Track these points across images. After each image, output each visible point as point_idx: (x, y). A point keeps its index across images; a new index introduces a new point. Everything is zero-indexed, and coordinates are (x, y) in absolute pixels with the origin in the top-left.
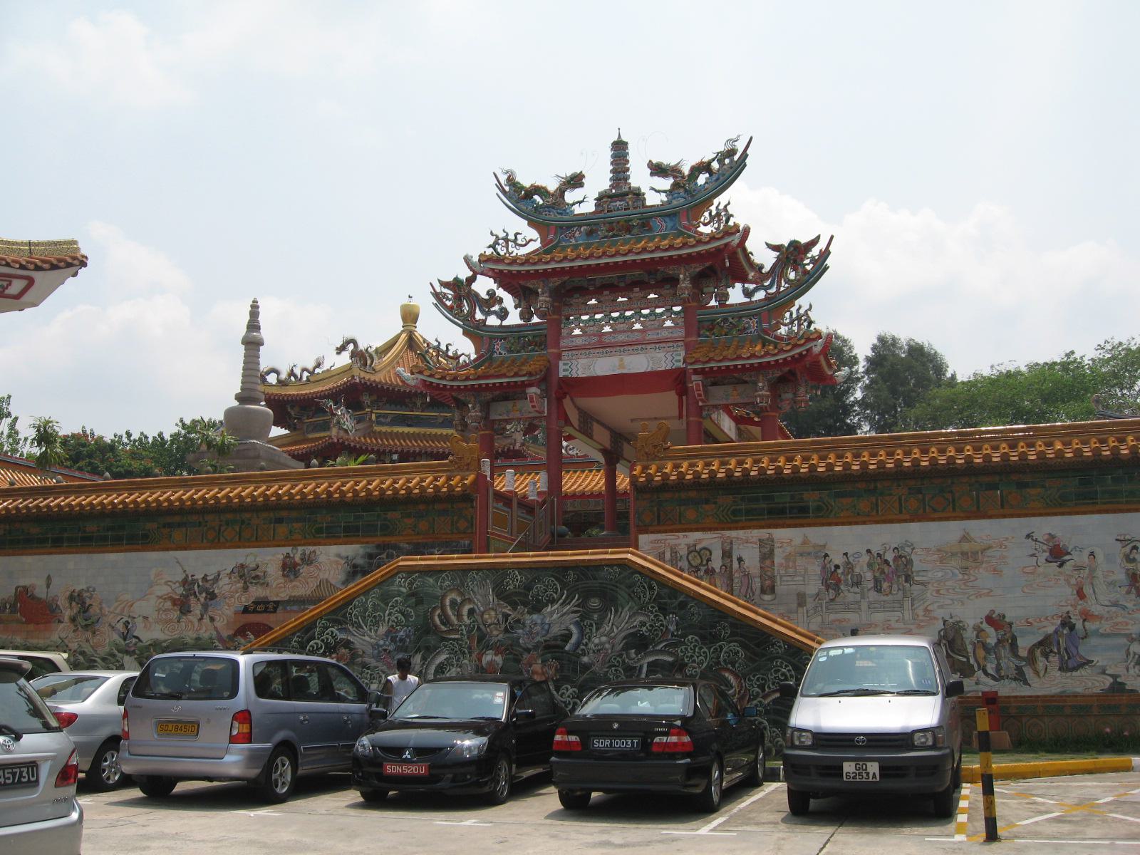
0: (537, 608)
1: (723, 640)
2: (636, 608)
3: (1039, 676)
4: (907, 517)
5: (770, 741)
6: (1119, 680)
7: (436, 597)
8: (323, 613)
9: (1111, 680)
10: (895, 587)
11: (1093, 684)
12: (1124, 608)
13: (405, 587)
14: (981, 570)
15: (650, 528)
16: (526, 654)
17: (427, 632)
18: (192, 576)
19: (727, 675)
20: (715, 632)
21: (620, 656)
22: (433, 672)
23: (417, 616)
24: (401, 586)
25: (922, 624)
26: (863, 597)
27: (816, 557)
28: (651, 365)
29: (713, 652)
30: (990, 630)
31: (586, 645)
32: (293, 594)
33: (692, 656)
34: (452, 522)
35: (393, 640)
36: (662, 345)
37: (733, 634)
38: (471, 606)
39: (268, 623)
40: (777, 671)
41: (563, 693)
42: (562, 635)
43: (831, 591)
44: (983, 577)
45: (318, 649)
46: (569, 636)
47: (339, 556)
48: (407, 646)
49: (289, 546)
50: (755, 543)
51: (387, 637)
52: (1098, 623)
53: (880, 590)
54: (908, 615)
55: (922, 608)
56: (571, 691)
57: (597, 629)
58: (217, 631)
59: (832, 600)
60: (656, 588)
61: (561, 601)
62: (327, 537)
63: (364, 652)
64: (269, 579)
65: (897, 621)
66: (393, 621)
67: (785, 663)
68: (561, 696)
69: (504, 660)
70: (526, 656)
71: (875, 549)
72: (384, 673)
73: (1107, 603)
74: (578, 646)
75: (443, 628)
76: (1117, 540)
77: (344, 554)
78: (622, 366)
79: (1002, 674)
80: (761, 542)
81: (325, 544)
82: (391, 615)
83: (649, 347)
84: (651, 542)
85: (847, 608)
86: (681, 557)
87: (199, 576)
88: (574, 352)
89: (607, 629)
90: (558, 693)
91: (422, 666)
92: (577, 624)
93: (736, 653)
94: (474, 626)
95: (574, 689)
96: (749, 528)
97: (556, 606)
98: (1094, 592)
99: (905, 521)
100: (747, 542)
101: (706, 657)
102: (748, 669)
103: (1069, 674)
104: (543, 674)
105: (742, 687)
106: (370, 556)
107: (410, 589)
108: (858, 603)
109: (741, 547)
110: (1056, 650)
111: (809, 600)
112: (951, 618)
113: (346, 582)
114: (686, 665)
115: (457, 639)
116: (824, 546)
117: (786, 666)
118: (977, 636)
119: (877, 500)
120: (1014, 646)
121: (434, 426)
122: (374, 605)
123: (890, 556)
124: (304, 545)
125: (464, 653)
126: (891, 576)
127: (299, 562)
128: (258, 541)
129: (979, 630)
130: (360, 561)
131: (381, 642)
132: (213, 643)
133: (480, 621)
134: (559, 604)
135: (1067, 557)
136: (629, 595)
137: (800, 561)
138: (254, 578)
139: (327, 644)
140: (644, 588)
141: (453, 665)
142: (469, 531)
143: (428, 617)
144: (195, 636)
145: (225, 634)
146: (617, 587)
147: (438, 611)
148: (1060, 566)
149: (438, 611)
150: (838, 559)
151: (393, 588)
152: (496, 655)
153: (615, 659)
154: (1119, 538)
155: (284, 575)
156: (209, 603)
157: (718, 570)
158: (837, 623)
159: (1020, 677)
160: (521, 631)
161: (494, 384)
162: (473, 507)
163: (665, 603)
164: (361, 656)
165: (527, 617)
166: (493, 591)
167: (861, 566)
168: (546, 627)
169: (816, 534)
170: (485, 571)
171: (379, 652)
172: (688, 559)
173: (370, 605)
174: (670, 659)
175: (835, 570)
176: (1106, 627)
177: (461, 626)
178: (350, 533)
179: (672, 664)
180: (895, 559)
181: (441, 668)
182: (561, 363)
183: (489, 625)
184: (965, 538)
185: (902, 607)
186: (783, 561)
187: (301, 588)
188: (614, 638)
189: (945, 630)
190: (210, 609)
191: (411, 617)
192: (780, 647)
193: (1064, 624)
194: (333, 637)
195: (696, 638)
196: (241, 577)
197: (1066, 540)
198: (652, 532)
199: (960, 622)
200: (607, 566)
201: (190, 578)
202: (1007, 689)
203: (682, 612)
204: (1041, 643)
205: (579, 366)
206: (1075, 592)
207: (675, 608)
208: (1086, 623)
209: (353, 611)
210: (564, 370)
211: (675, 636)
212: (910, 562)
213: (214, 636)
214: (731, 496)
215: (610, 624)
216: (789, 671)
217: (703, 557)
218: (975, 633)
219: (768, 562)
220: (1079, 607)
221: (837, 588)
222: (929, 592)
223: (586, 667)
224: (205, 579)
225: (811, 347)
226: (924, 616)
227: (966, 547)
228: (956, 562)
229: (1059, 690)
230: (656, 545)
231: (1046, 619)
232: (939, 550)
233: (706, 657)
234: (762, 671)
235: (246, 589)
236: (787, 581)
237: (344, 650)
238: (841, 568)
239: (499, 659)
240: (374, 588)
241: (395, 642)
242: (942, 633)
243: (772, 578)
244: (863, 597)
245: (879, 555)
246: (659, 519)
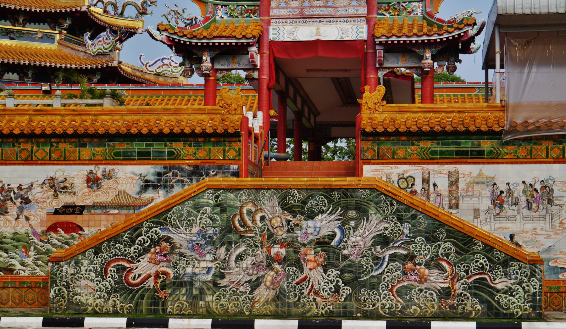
0: (311, 216)
2: (382, 218)
4: (552, 160)
5: (471, 307)
7: (237, 208)
8: (149, 217)
10: (541, 206)
13: (212, 199)
15: (372, 161)
16: (303, 247)
17: (230, 232)
18: (8, 185)
19: (443, 263)
21: (370, 250)
22: (234, 259)
23: (222, 220)
24: (209, 199)
25: (558, 232)
26: (518, 213)
27: (488, 185)
28: (341, 34)
29: (434, 249)
31: (346, 242)
32: (96, 201)
33: (419, 251)
34: (224, 151)
35: (204, 236)
36: (349, 19)
37: (448, 237)
38: (262, 214)
39: (75, 222)
40: (477, 262)
41: (330, 274)
42: (329, 235)
43: (497, 208)
45: (144, 243)
46: (334, 236)
47: (133, 173)
48: (214, 241)
49: (92, 164)
50: (446, 174)
51: (199, 234)
53: (531, 208)
54: (549, 226)
55: (558, 221)
56: (335, 273)
57: (354, 232)
58: (32, 227)
59: (498, 214)
60: (395, 205)
61: (328, 212)
62: (124, 160)
63: (181, 245)
64: (75, 190)
65: (541, 229)
66: (204, 224)
68: (328, 276)
69: (287, 252)
70: (303, 249)
71: (528, 182)
72: (197, 260)
74: (340, 243)
75: (242, 229)
77: (138, 172)
78: (318, 33)
81: (122, 164)
82: (202, 220)
83: (339, 20)
84: (372, 171)
85: (508, 220)
86: (393, 182)
87: (14, 186)
88: (280, 20)
89: (361, 231)
90: (326, 274)
91: (226, 255)
92: (339, 227)
94: (265, 228)
95: (338, 272)
96: (442, 163)
97: (325, 215)
99: (550, 163)
101: (429, 252)
104: (315, 261)
105: (453, 271)
106: (159, 174)
107: (216, 201)
108: (515, 217)
111: (482, 214)
113: (140, 193)
114: (416, 256)
115: (253, 237)
116: (494, 178)
117: (483, 258)
119: (531, 147)
121: (33, 40)
122: (189, 212)
123: (538, 186)
124: (105, 164)
125: (257, 246)
126: (538, 199)
127: (101, 177)
128: (65, 160)
130: (151, 178)
131: (195, 238)
132: (29, 237)
133: (269, 224)
134: (326, 214)
136: (377, 209)
137: (477, 188)
138: (63, 188)
139: (152, 239)
140: (387, 204)
141: (249, 255)
142: (237, 158)
143: (230, 221)
144: (13, 231)
145: (39, 230)
146: (368, 203)
147: (238, 217)
149: (238, 217)
151: (202, 200)
152: (281, 248)
153: (366, 252)
155: (88, 187)
156: (24, 206)
157: (419, 192)
160: (299, 232)
161: (225, 43)
162: (240, 141)
163: (402, 215)
164: (180, 248)
165: (304, 222)
166: (279, 203)
167: (518, 192)
168: (318, 229)
170: (273, 190)
171: (193, 245)
172: (398, 183)
173: (185, 212)
174: (405, 252)
175: (500, 194)
177: (255, 228)
178: (144, 157)
179: (406, 256)
180: (542, 188)
181: (241, 257)
182: (271, 28)
183: (276, 228)
185: (545, 220)
186: (465, 187)
187: (103, 196)
188: (366, 237)
190: (25, 211)
191: (217, 221)
192: (479, 246)
194: (157, 235)
195: (423, 239)
196: (51, 187)
198: (374, 164)
200: (361, 189)
201: (7, 187)
203: (414, 221)
205: (285, 31)
207: (408, 218)
209: (173, 216)
210: (274, 34)
211: (409, 237)
212: (551, 190)
213: (29, 232)
214: (430, 141)
215: (363, 228)
216: (485, 261)
217: (409, 182)
219: (454, 187)
221: (501, 206)
223: (346, 257)
224: (20, 188)
225: (468, 30)
226: (560, 226)
230: (376, 173)
233: (429, 252)
234: (467, 261)
235: (56, 196)
236: (467, 201)
237: (165, 244)
238: (505, 193)
239: (283, 251)
240: (188, 200)
241: (205, 239)
243: (457, 198)
244: (518, 213)
245: (531, 185)
246: (378, 156)
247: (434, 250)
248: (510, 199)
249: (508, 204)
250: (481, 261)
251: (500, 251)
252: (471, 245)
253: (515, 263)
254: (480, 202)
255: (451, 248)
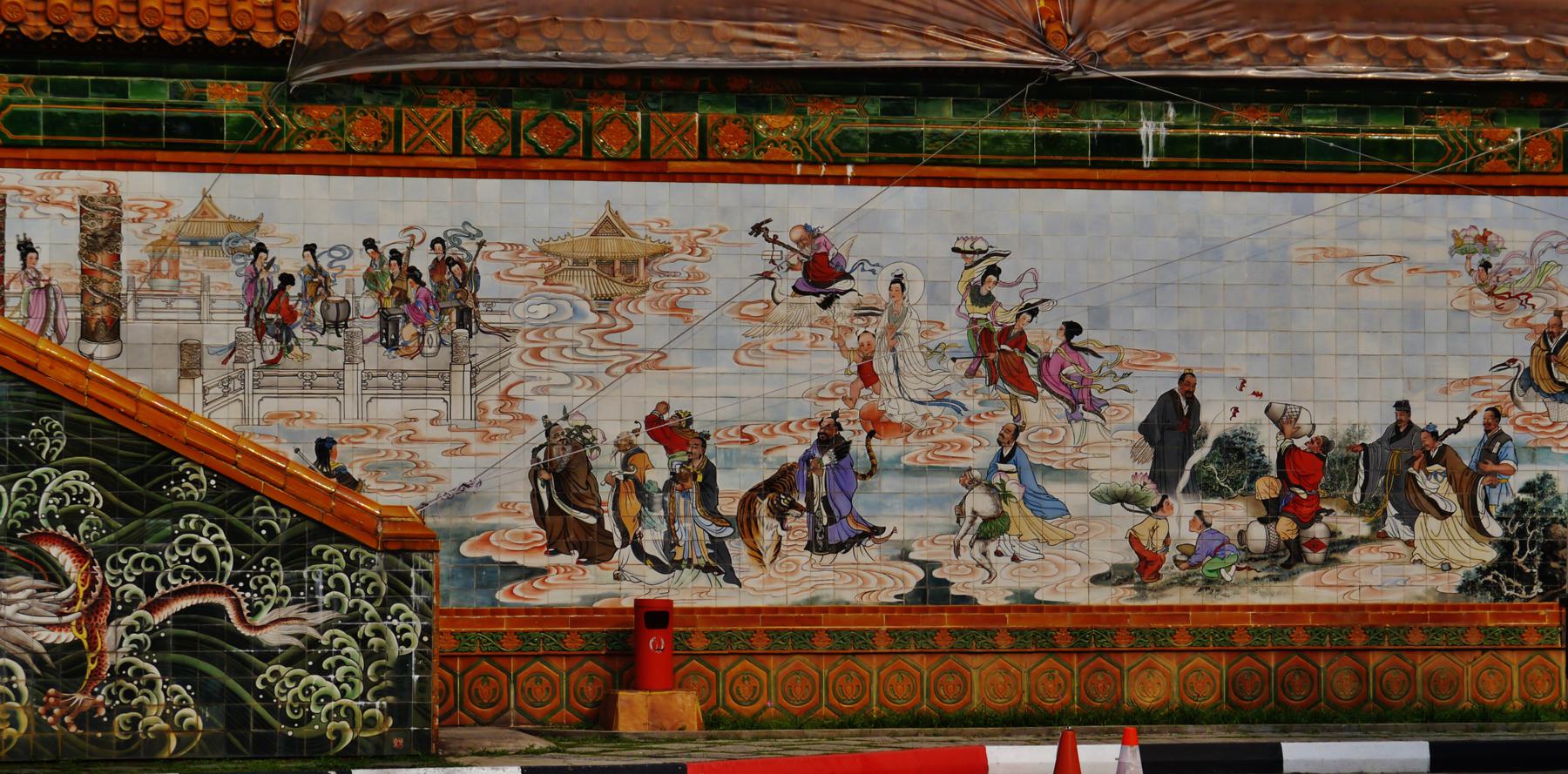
1: (47, 462)
3: (761, 561)
4: (472, 163)
5: (164, 717)
6: (936, 574)
9: (921, 574)
10: (432, 334)
11: (880, 581)
12: (959, 408)
14: (641, 306)
19: (54, 551)
20: (26, 443)
25: (494, 431)
27: (234, 252)
29: (19, 494)
30: (657, 454)
40: (186, 544)
43: (268, 340)
44: (647, 325)
50: (70, 206)
52: (900, 441)
54: (461, 408)
55: (495, 391)
59: (273, 363)
65: (434, 422)
67: (209, 524)
71: (388, 239)
73: (923, 396)
76: (955, 250)
79: (678, 557)
80: (87, 206)
85: (308, 384)
93: (79, 497)
96: (55, 164)
98: (897, 368)
99: (465, 173)
100: (47, 202)
102: (112, 536)
103: (829, 558)
105: (94, 581)
108: (337, 373)
109: (30, 213)
110: (802, 502)
111: (210, 361)
112: (566, 418)
117: (212, 531)
118: (625, 466)
119: (398, 114)
120: (708, 492)
123: (422, 260)
126: (422, 308)
129: (630, 452)
135: (841, 285)
137: (190, 260)
148: (825, 305)
150: (290, 260)
154: (960, 245)
158: (281, 421)
159: (719, 563)
167: (349, 281)
169: (239, 193)
175: (282, 288)
176: (916, 452)
180: (438, 267)
184: (610, 225)
185: (447, 386)
186: (145, 257)
189: (548, 446)
192: (197, 483)
193: (824, 442)
197: (846, 246)
199: (586, 428)
202: (690, 591)
204: (769, 487)
206: (854, 368)
208: (874, 441)
212: (471, 277)
216: (218, 542)
218: (620, 456)
219: (102, 259)
220: (861, 404)
221: (283, 332)
222: (515, 352)
226: (501, 411)
227: (610, 246)
228: (583, 283)
229: (805, 596)
231: (786, 427)
232: (543, 251)
234: (148, 543)
236: (154, 310)
242: (541, 455)
243: (114, 301)
244: (349, 361)
245: (395, 255)
247: (17, 502)
248: (318, 306)
249: (311, 327)
250: (204, 541)
251: (276, 505)
252: (166, 481)
253: (331, 550)
254: (205, 316)
255: (87, 493)
